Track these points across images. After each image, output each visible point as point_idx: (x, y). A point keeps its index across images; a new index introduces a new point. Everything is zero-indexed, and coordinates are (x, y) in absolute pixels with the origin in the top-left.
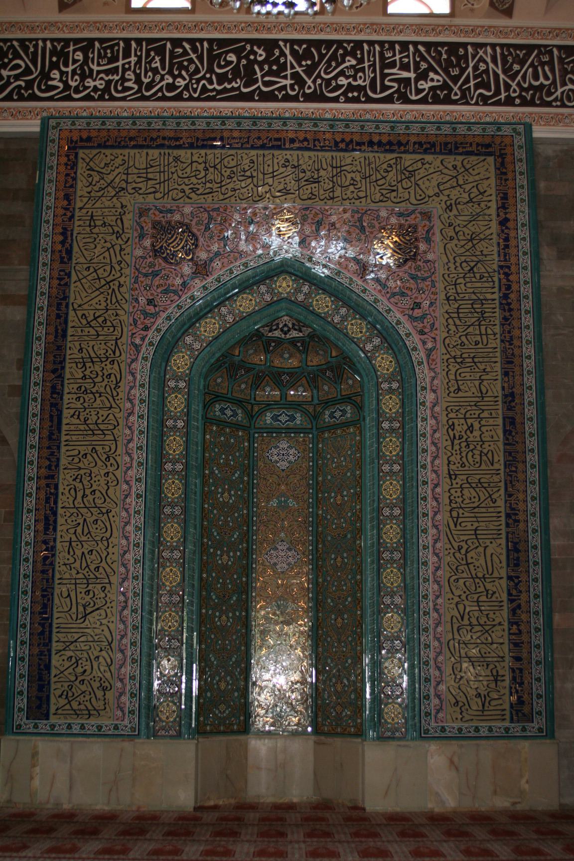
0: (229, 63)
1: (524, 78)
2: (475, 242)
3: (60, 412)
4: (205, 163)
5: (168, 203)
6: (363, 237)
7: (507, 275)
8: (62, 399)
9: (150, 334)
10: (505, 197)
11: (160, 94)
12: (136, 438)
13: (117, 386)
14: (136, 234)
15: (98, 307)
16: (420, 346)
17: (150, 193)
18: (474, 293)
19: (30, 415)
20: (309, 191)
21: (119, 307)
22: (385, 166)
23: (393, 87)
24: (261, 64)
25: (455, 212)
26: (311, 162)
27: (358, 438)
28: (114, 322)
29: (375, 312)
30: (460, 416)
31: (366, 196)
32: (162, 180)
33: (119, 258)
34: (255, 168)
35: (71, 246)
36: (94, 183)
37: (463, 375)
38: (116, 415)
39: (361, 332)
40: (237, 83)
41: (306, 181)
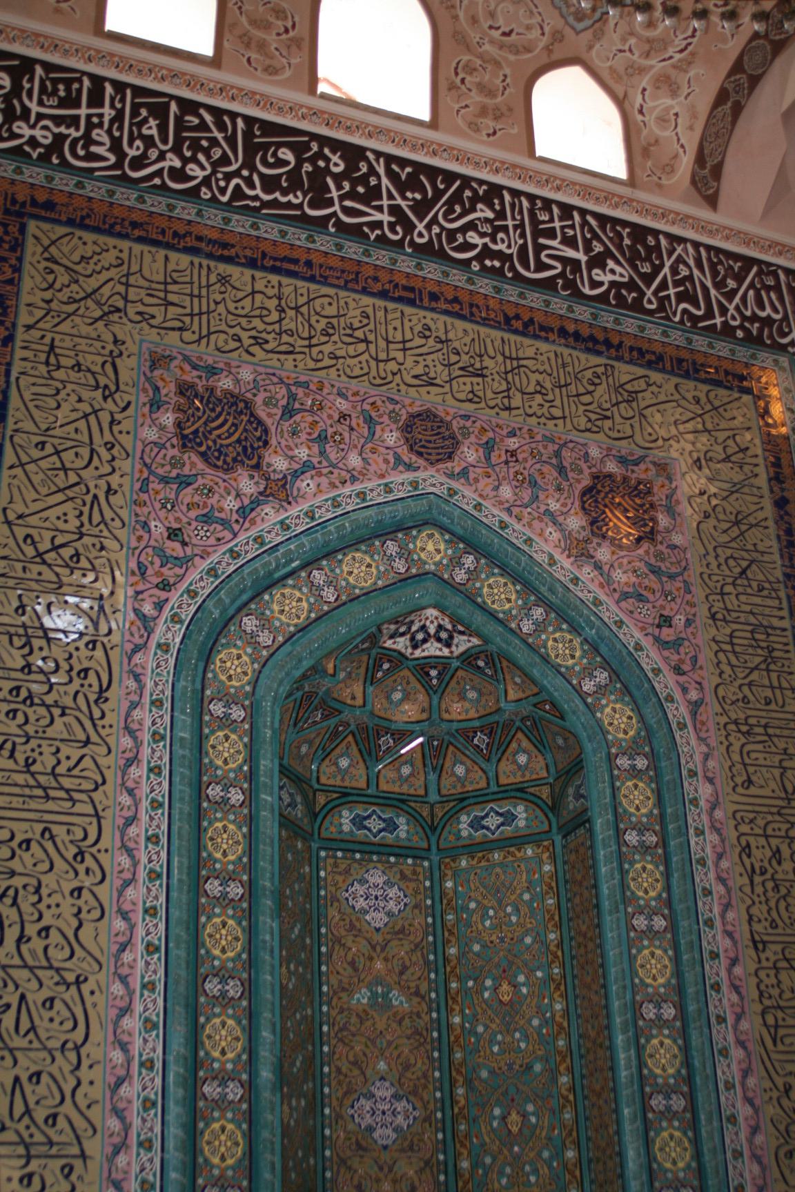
2: (744, 528)
4: (280, 299)
5: (207, 353)
6: (565, 484)
9: (174, 597)
11: (157, 181)
12: (144, 818)
13: (102, 696)
14: (143, 399)
16: (677, 695)
17: (173, 329)
20: (468, 388)
21: (106, 533)
23: (555, 268)
24: (338, 179)
26: (467, 340)
28: (97, 562)
31: (564, 418)
32: (196, 311)
34: (371, 326)
36: (57, 286)
37: (753, 755)
38: (100, 761)
39: (573, 657)
40: (296, 197)
41: (462, 369)
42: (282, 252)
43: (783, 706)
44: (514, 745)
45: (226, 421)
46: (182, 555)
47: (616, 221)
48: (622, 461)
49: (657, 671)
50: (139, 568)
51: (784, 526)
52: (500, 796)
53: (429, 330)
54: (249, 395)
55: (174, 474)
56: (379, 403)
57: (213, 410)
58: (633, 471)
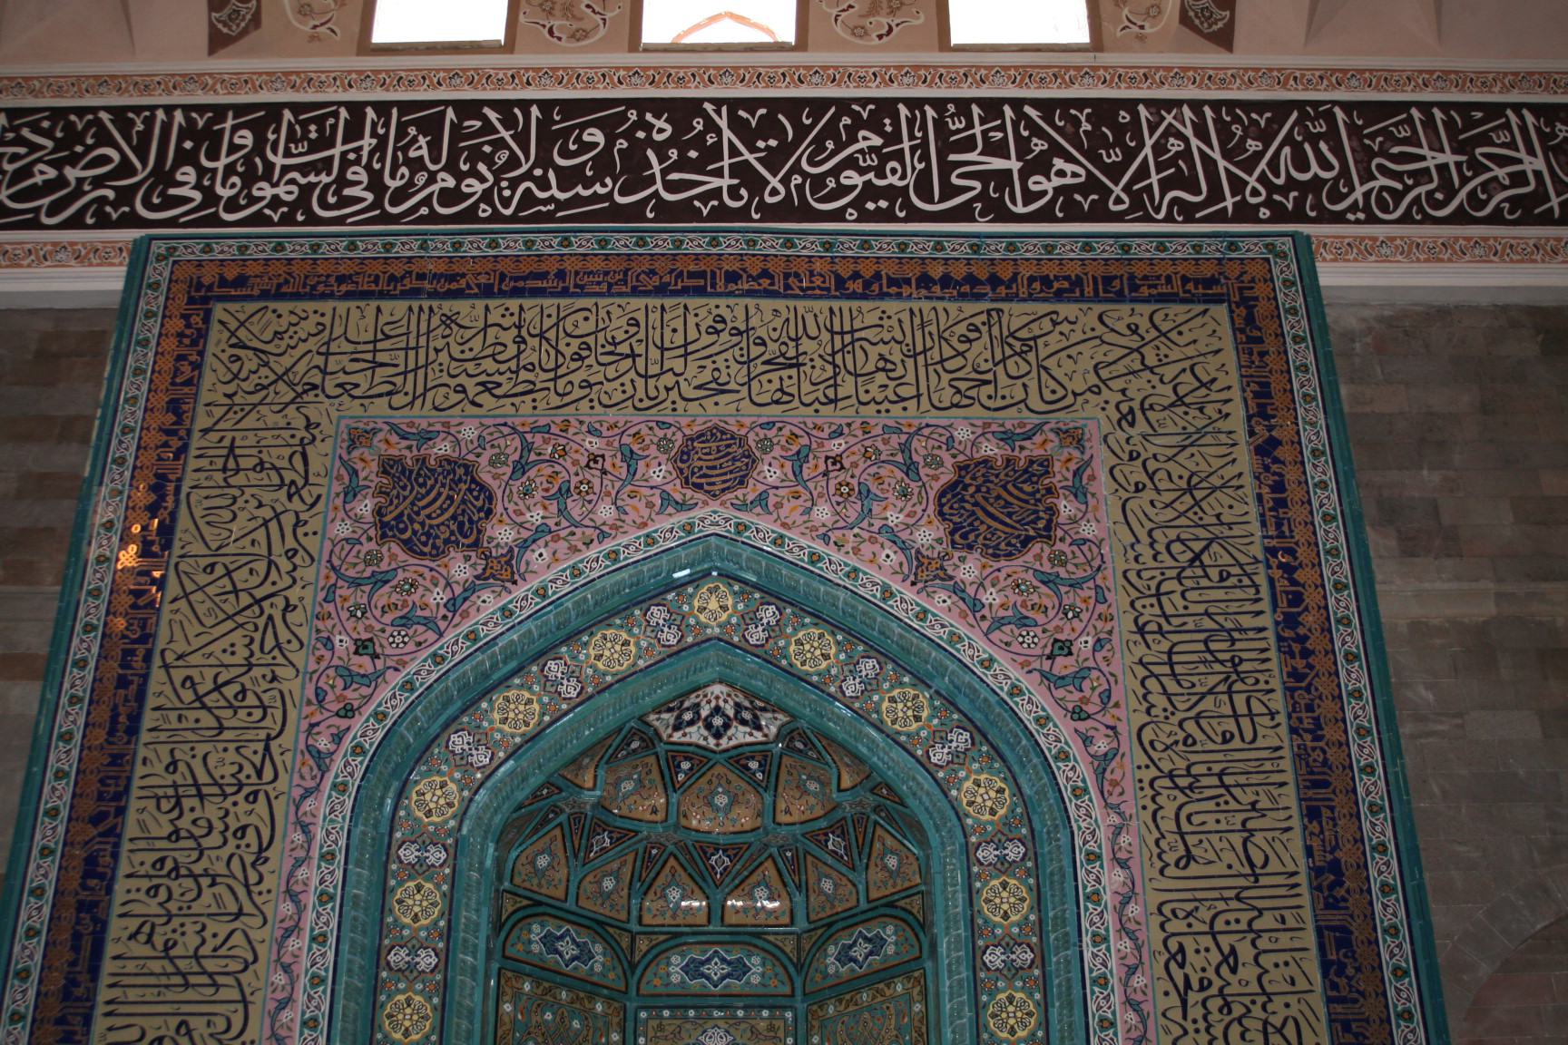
0: (586, 147)
1: (1274, 165)
2: (1199, 494)
3: (101, 926)
4: (519, 327)
5: (422, 416)
7: (1288, 569)
8: (109, 890)
9: (357, 724)
10: (1263, 392)
12: (301, 998)
13: (261, 857)
15: (227, 659)
16: (1075, 749)
17: (380, 395)
18: (1207, 613)
19: (21, 931)
20: (776, 385)
21: (280, 660)
22: (961, 329)
24: (661, 150)
25: (1141, 426)
26: (778, 323)
27: (917, 1007)
28: (265, 697)
29: (953, 666)
30: (1198, 927)
31: (918, 396)
32: (411, 366)
33: (290, 543)
34: (642, 335)
35: (173, 515)
36: (242, 376)
37: (1195, 819)
38: (252, 935)
39: (917, 719)
42: (525, 269)
43: (1254, 740)
44: (877, 845)
45: (439, 494)
46: (371, 670)
47: (1066, 104)
48: (1006, 437)
49: (1043, 721)
50: (317, 695)
51: (1271, 480)
52: (869, 915)
53: (724, 321)
54: (471, 457)
55: (368, 573)
56: (645, 431)
57: (423, 485)
58: (1022, 448)
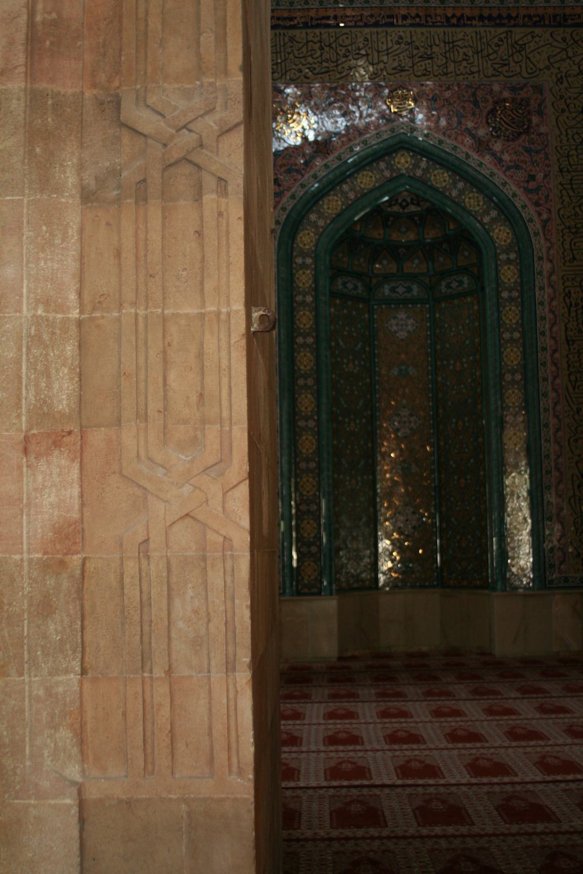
4: (320, 42)
6: (477, 111)
16: (535, 218)
20: (423, 67)
22: (496, 40)
25: (565, 84)
30: (576, 284)
31: (479, 71)
41: (420, 57)
53: (402, 38)
